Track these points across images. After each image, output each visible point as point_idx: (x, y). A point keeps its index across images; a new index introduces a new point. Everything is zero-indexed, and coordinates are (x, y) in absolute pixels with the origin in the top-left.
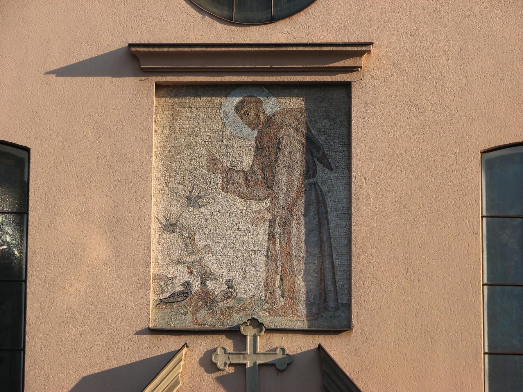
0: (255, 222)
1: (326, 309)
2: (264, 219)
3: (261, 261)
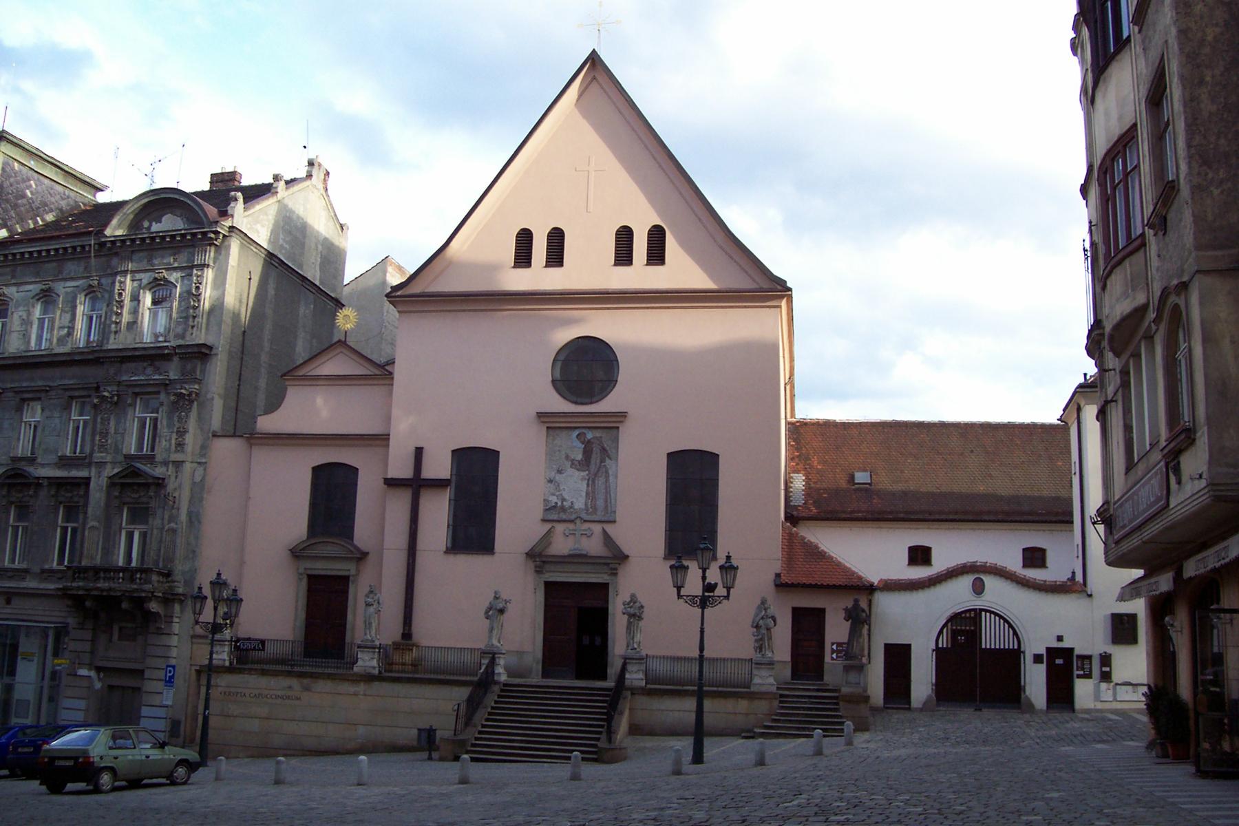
0: (583, 479)
1: (607, 513)
2: (585, 479)
3: (584, 494)
